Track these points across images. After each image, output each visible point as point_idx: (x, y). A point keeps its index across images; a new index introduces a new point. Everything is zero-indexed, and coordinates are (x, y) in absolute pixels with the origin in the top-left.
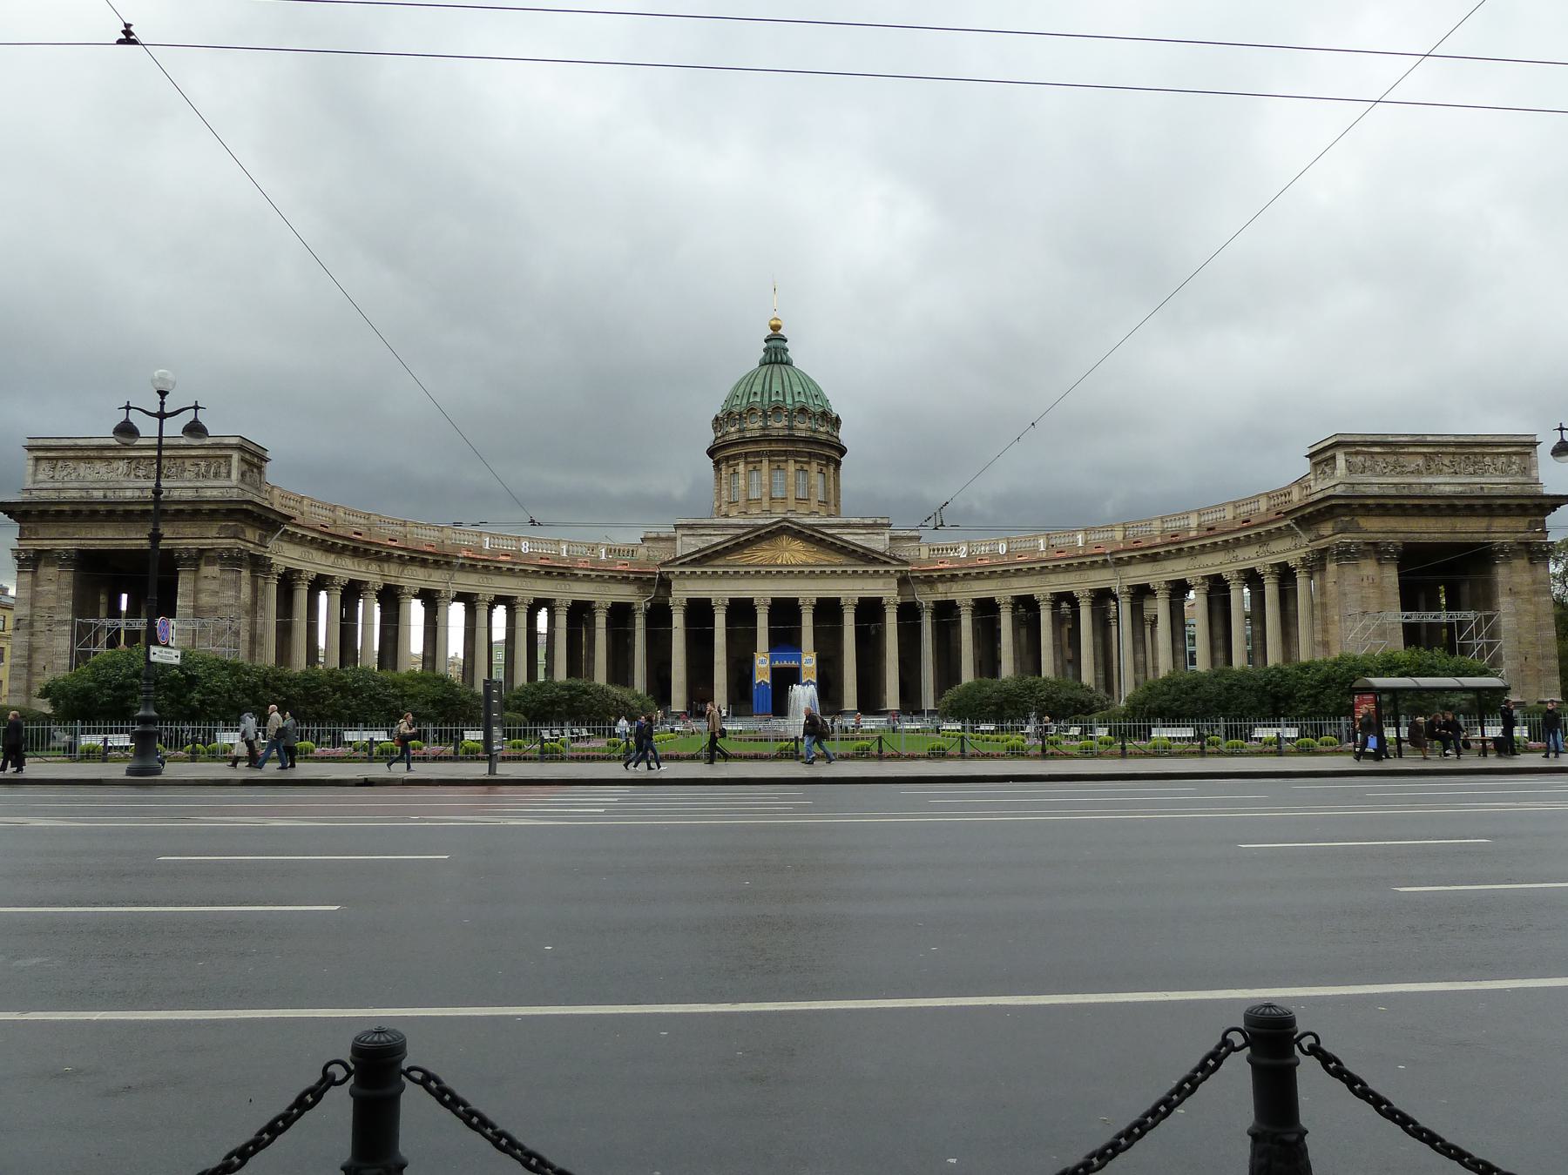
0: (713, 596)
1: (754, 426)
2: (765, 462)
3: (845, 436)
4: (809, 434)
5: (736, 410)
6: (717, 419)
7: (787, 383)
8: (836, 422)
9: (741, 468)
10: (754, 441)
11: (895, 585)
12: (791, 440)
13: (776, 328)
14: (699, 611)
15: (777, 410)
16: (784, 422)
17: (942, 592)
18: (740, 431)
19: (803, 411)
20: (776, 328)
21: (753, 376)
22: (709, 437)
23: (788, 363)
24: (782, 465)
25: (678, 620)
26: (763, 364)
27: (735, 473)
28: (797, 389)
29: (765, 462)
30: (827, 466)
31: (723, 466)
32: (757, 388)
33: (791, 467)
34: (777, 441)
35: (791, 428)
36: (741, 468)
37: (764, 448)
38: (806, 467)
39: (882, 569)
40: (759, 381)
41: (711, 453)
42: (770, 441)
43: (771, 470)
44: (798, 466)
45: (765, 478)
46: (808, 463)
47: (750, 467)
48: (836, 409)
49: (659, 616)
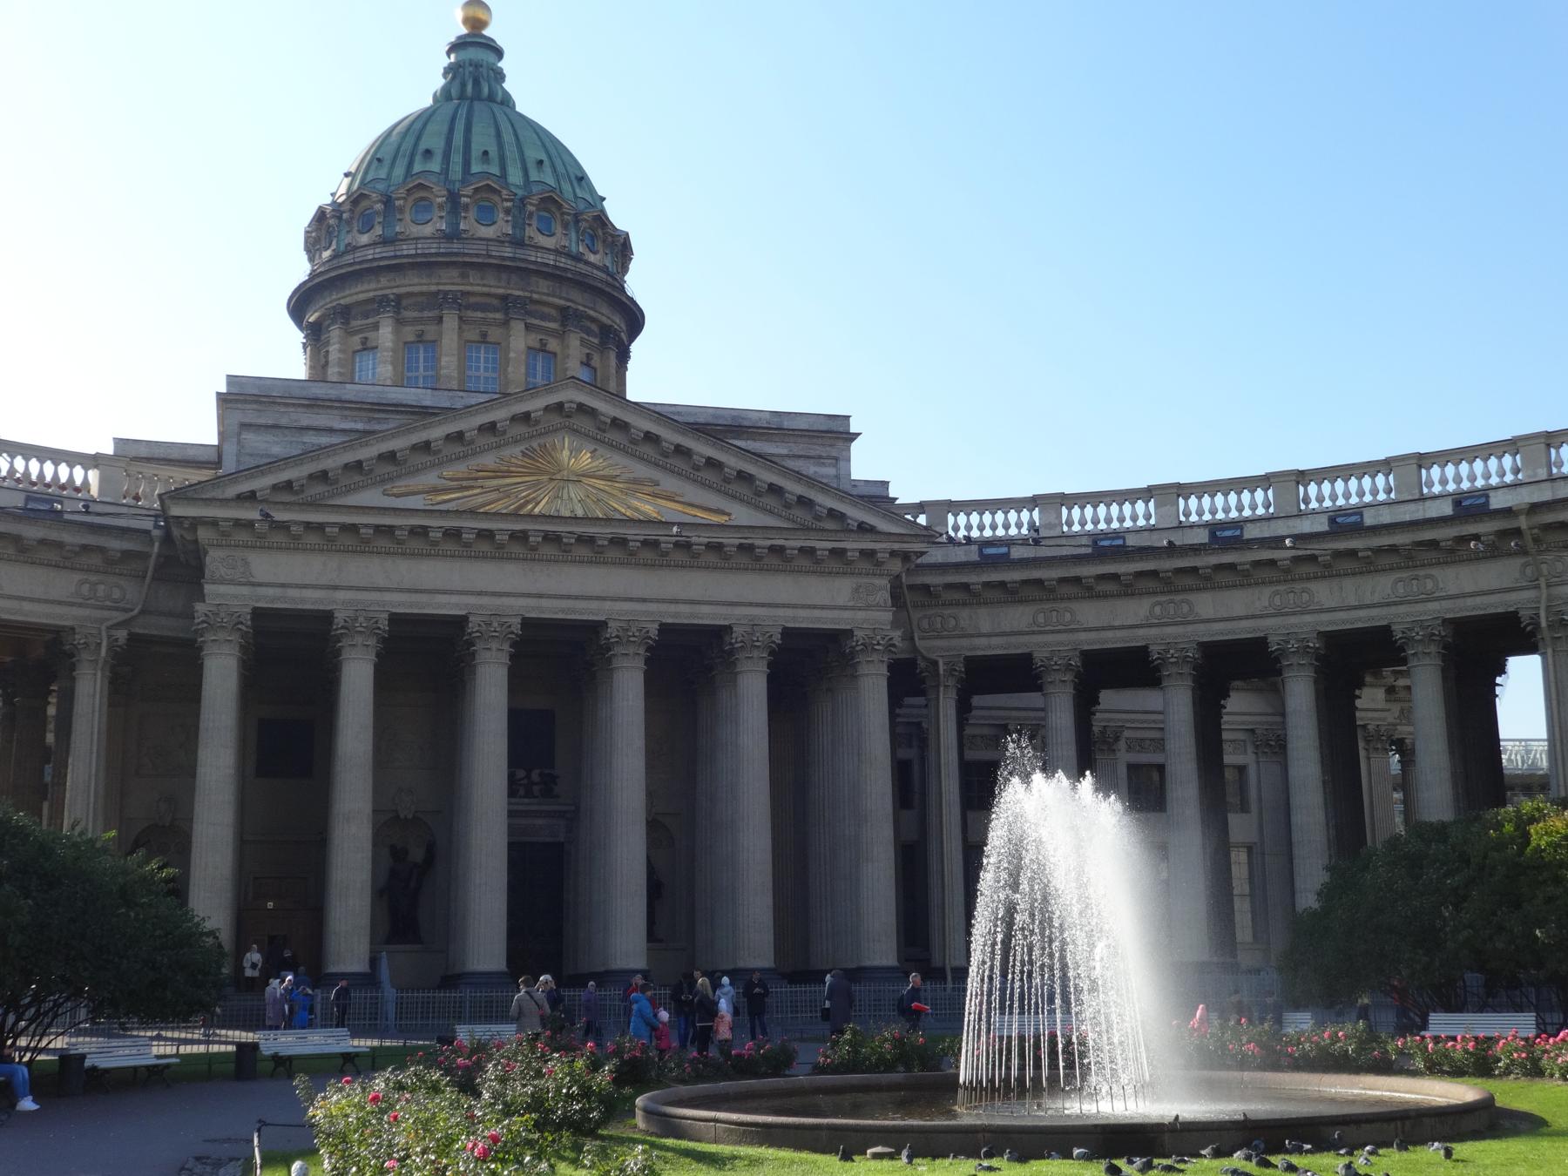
0: (340, 604)
1: (425, 230)
2: (451, 321)
3: (636, 283)
4: (564, 262)
5: (381, 186)
6: (321, 216)
7: (508, 137)
8: (621, 248)
9: (385, 334)
10: (425, 265)
11: (884, 596)
12: (524, 272)
13: (476, 24)
14: (291, 657)
15: (488, 191)
16: (502, 226)
17: (997, 629)
18: (385, 241)
19: (550, 202)
20: (476, 24)
21: (423, 120)
22: (299, 269)
23: (507, 101)
24: (495, 334)
25: (221, 675)
26: (444, 96)
27: (367, 347)
28: (533, 154)
29: (451, 321)
30: (603, 347)
31: (335, 333)
32: (433, 140)
33: (519, 340)
34: (481, 267)
35: (519, 243)
36: (385, 334)
37: (449, 281)
38: (553, 345)
39: (853, 545)
40: (438, 128)
41: (299, 305)
42: (466, 267)
43: (465, 344)
44: (533, 339)
45: (449, 362)
46: (561, 335)
47: (409, 333)
48: (618, 216)
49: (155, 675)
